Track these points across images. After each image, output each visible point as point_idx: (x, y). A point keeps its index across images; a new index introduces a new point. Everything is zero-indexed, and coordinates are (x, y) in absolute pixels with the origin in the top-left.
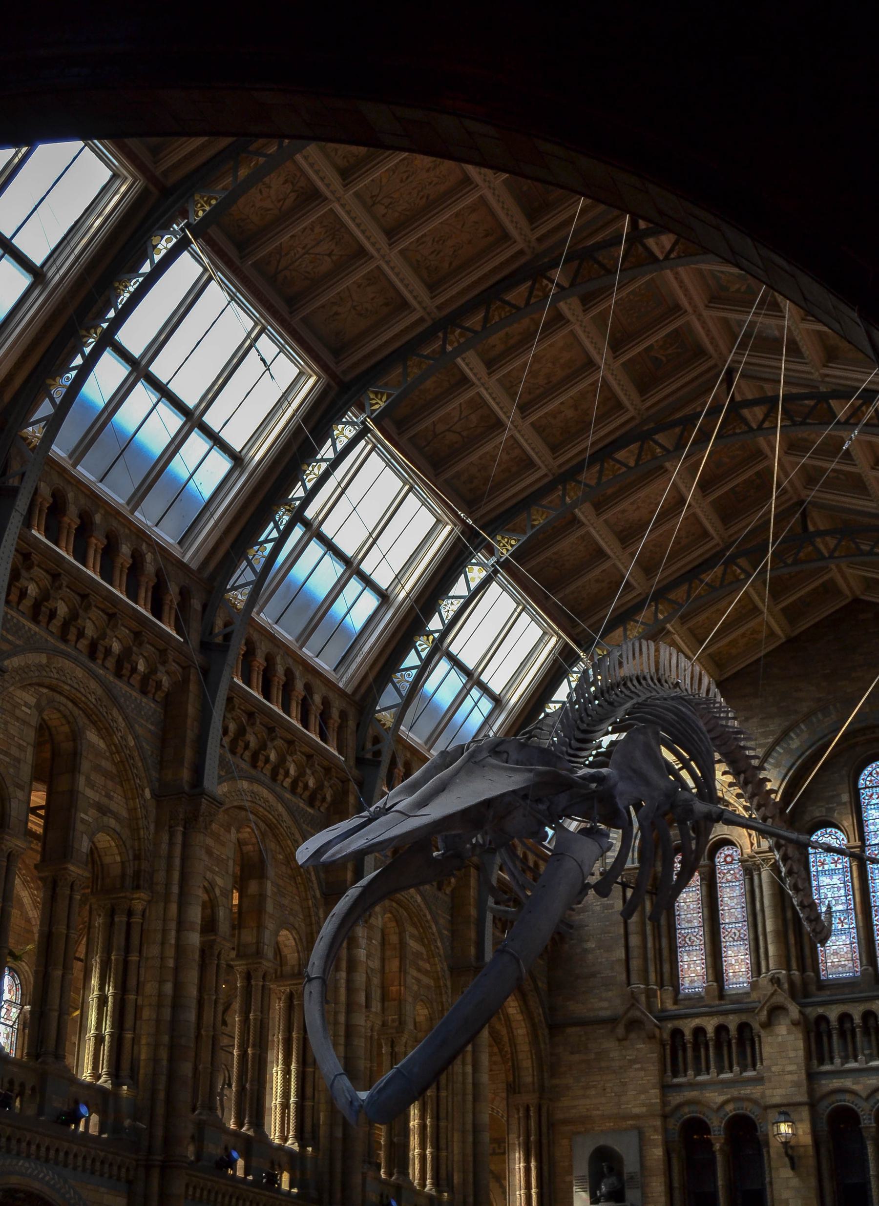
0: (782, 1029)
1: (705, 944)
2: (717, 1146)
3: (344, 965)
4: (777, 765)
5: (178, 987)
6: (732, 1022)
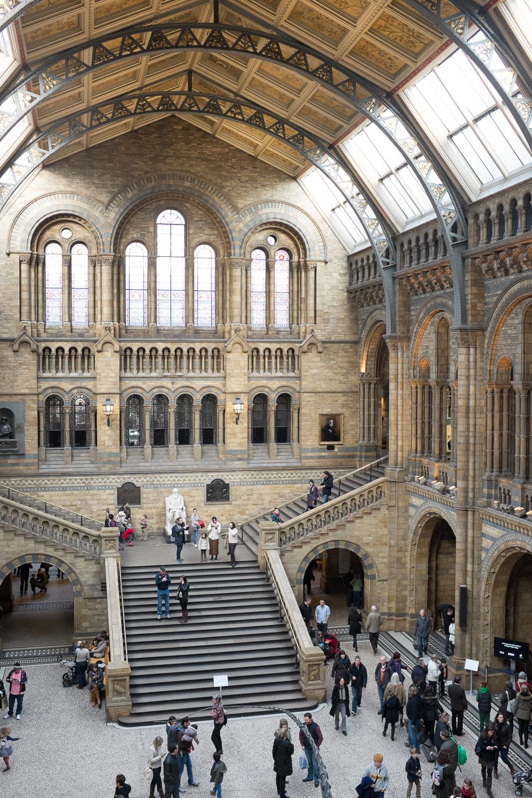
2: (67, 411)
4: (118, 206)
6: (80, 346)
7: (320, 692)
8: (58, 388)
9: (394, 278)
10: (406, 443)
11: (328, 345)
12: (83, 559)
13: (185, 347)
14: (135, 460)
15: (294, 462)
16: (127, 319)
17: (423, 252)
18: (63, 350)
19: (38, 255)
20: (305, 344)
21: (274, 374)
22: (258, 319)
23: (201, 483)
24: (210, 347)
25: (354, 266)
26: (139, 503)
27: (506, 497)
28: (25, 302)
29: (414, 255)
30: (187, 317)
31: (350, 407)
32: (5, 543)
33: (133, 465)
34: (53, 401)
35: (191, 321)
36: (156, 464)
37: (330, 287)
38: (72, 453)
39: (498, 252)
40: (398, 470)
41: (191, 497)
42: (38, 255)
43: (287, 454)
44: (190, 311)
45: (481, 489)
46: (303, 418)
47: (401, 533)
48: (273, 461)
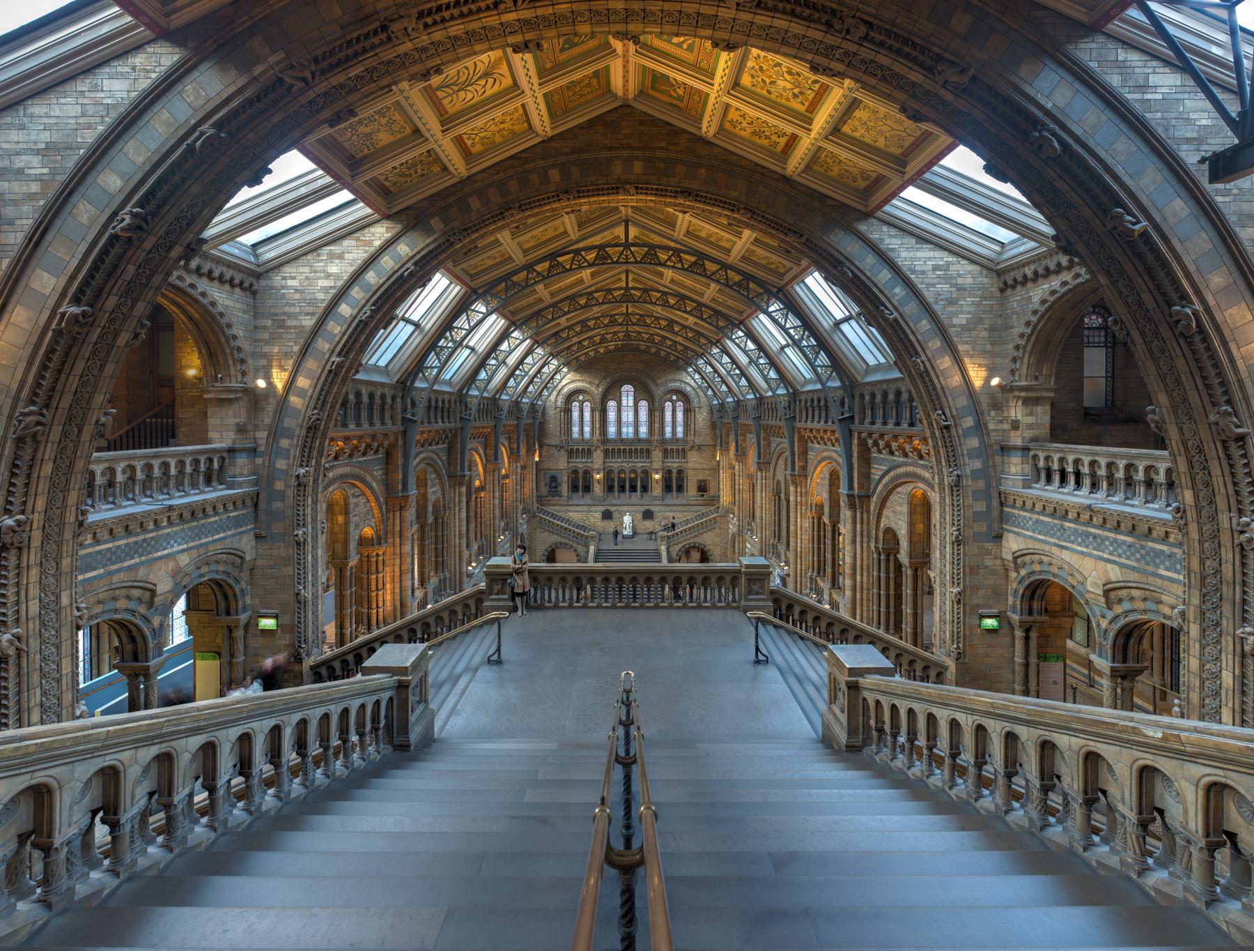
6: (586, 448)
13: (633, 448)
24: (645, 448)
34: (575, 472)
44: (636, 431)
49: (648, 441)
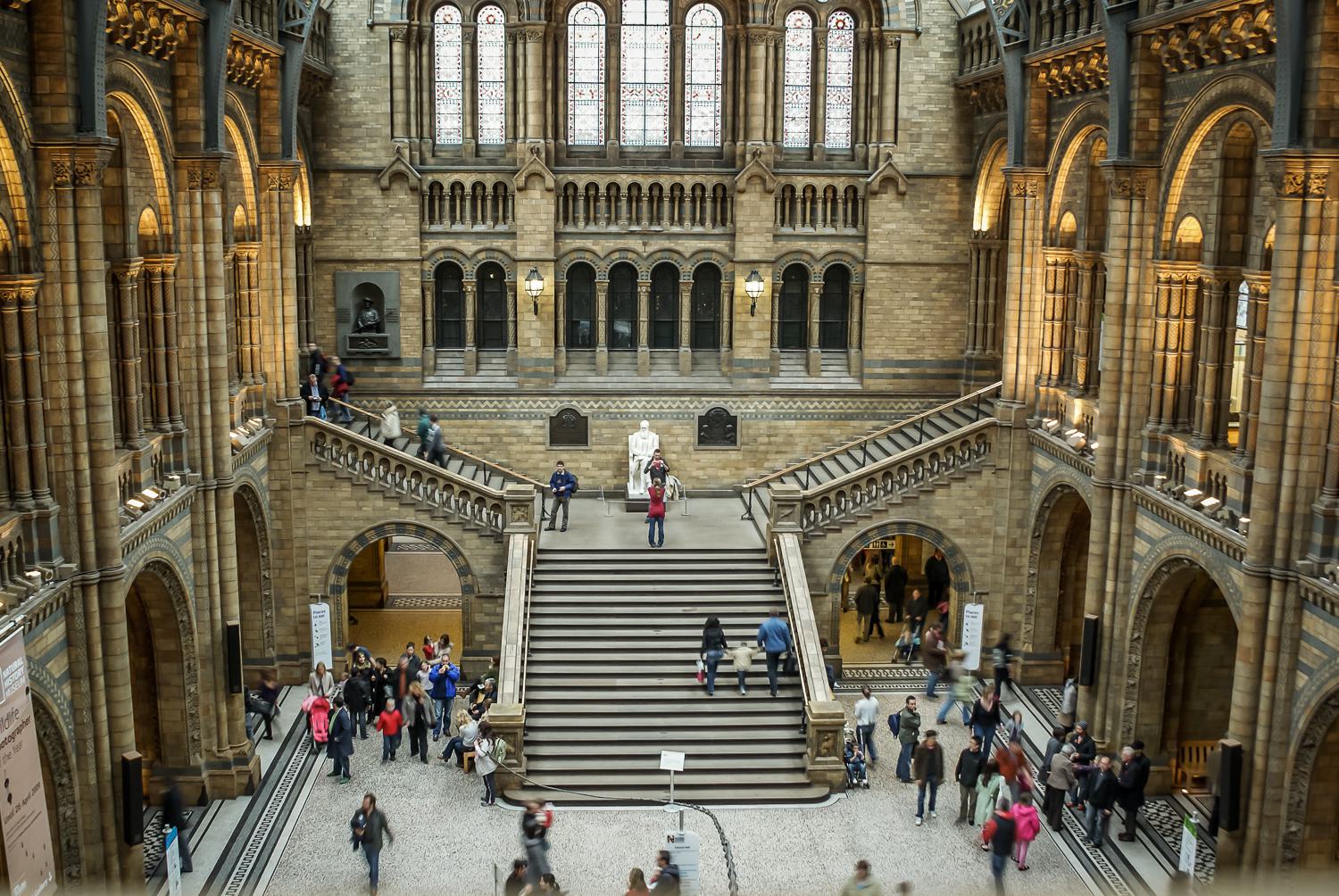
0: (536, 193)
1: (463, 99)
2: (469, 288)
3: (200, 237)
5: (88, 381)
6: (490, 180)
7: (835, 775)
8: (454, 250)
9: (1024, 67)
10: (1035, 360)
11: (917, 181)
12: (474, 535)
13: (666, 181)
14: (579, 376)
15: (850, 384)
16: (570, 133)
17: (1071, 19)
18: (463, 188)
19: (420, 27)
20: (875, 180)
21: (820, 230)
22: (796, 133)
23: (689, 414)
24: (710, 182)
25: (967, 41)
26: (586, 443)
27: (1176, 470)
28: (400, 107)
29: (1058, 24)
30: (672, 130)
31: (955, 292)
32: (353, 503)
33: (575, 380)
35: (678, 136)
36: (615, 379)
37: (923, 78)
38: (478, 358)
39: (1185, 27)
40: (1015, 406)
41: (673, 435)
42: (420, 27)
43: (839, 368)
45: (1138, 453)
46: (868, 308)
47: (1017, 515)
48: (813, 380)
49: (724, 159)
